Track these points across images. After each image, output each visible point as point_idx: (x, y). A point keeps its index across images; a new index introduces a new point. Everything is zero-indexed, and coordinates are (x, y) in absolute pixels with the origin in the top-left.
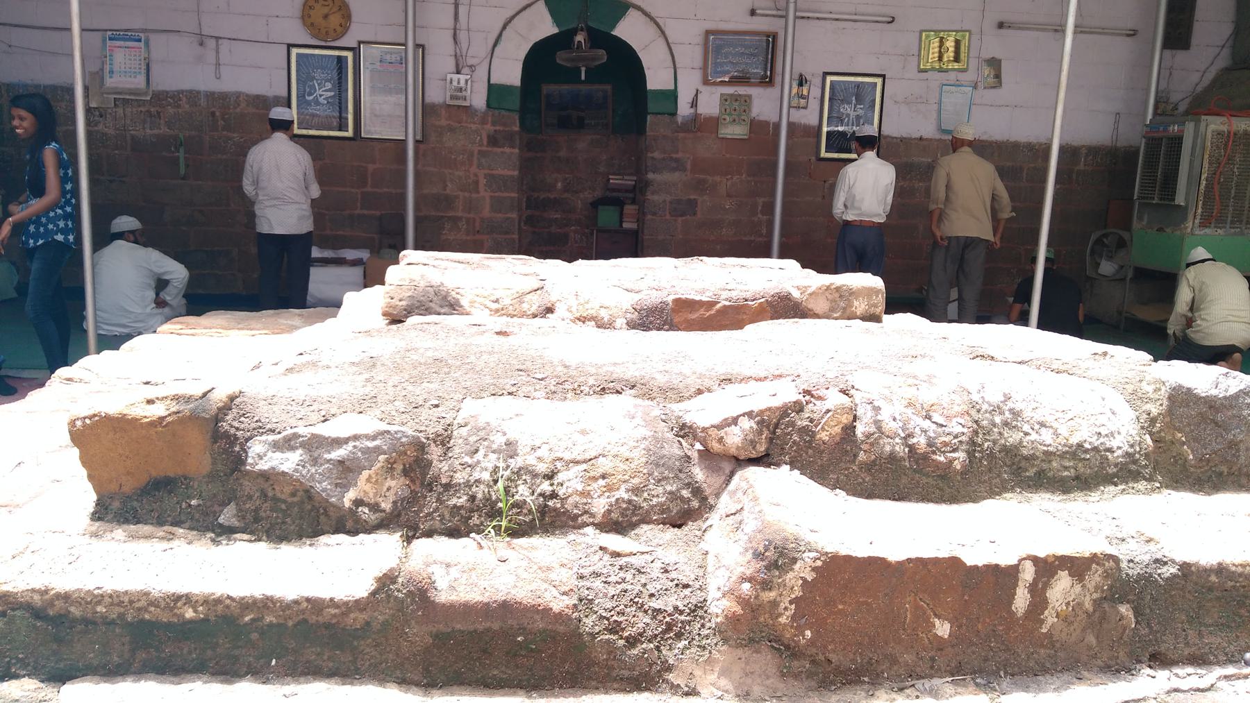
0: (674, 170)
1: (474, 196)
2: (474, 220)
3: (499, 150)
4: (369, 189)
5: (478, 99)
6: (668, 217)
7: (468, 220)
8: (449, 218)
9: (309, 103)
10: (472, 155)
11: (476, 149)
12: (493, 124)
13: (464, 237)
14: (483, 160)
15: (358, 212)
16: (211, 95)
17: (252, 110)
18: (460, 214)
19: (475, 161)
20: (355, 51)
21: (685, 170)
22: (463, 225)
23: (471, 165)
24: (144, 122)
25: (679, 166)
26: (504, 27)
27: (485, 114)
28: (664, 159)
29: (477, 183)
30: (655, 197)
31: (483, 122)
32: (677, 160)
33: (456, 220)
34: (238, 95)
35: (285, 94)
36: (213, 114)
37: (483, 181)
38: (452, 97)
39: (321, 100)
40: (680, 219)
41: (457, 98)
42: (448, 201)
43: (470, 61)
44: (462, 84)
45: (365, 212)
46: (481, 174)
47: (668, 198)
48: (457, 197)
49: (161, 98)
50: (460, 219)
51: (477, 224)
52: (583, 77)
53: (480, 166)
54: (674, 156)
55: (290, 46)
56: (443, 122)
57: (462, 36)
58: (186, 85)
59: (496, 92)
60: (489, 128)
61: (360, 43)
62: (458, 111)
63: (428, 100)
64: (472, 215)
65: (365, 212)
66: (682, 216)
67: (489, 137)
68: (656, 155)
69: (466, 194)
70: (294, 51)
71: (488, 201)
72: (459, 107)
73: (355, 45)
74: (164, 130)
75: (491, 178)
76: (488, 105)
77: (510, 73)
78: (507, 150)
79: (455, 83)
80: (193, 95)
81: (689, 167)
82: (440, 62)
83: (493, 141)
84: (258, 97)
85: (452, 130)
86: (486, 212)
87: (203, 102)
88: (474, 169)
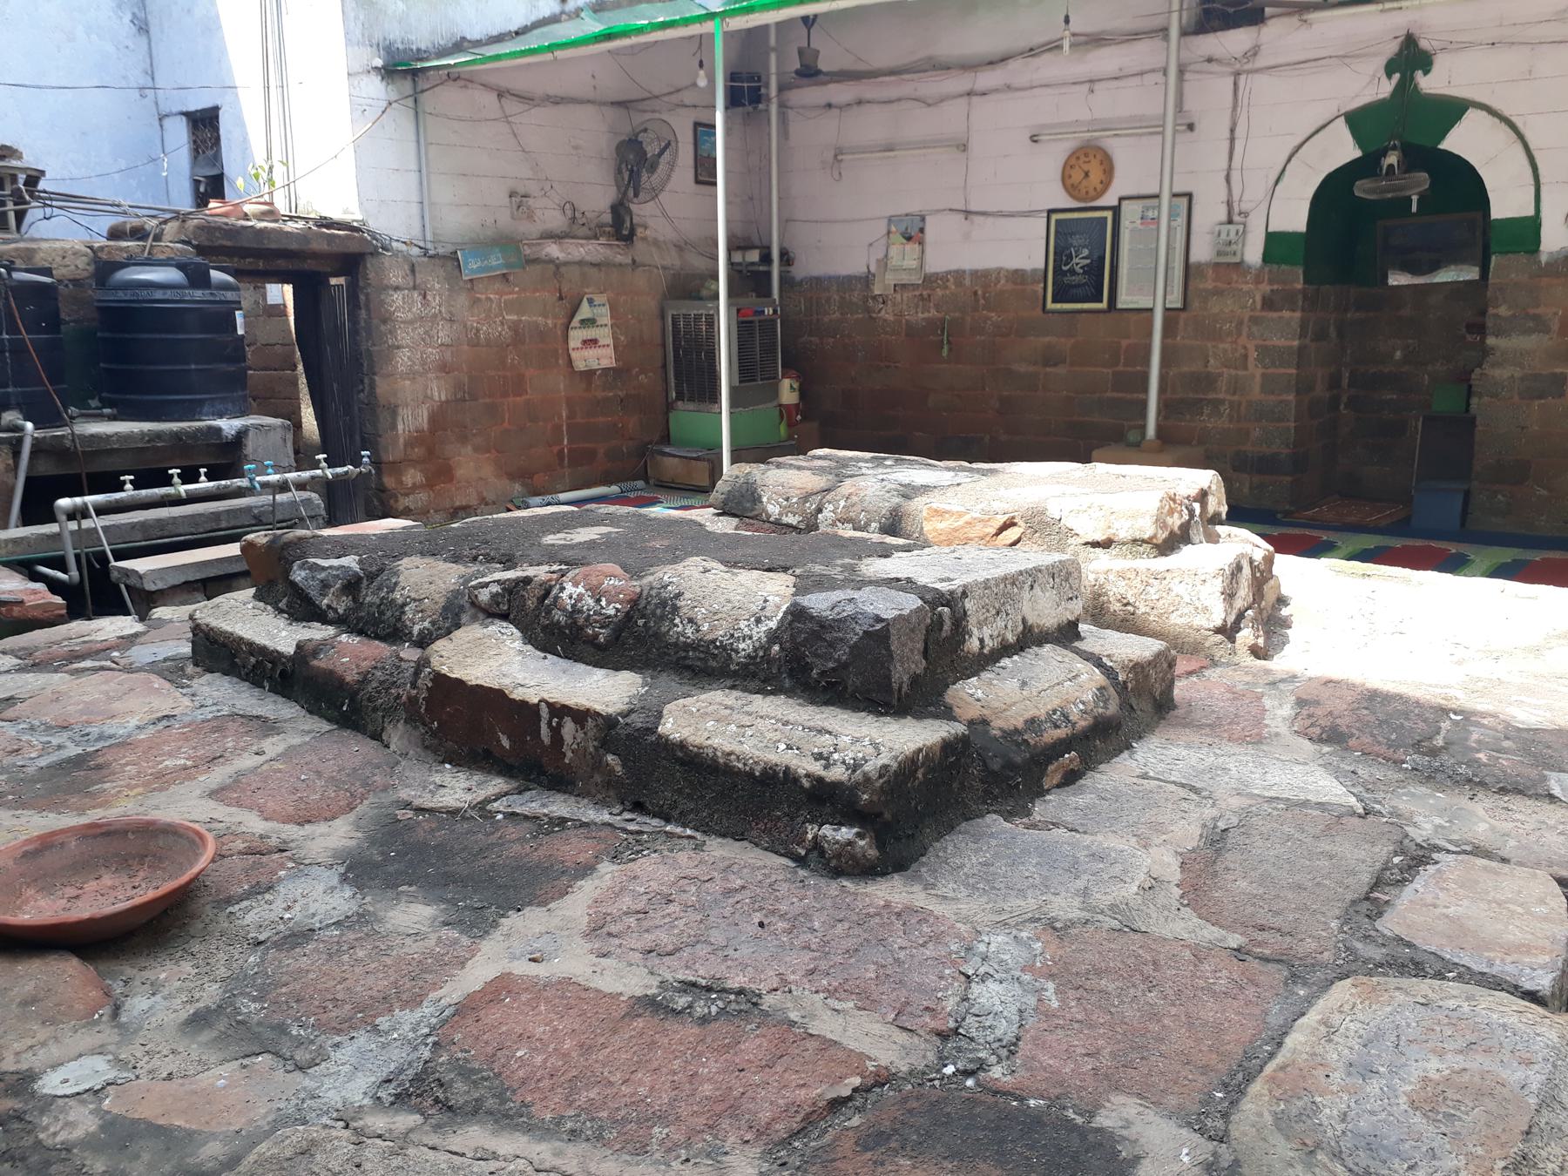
0: (1527, 332)
1: (1241, 373)
2: (1240, 404)
3: (1275, 315)
4: (1120, 368)
5: (1253, 253)
6: (1516, 398)
7: (1231, 403)
8: (1209, 401)
9: (1064, 273)
10: (1241, 323)
11: (1247, 314)
12: (1271, 282)
13: (1226, 426)
14: (1254, 329)
15: (1109, 394)
16: (975, 274)
17: (1010, 287)
18: (1221, 396)
19: (1245, 330)
20: (1116, 210)
21: (1547, 331)
22: (1225, 409)
23: (1239, 334)
24: (917, 306)
25: (1540, 325)
26: (1289, 160)
27: (1262, 268)
28: (1514, 316)
29: (1246, 357)
30: (1497, 373)
31: (1258, 280)
32: (1536, 318)
33: (1216, 403)
34: (999, 270)
35: (1042, 266)
36: (975, 293)
37: (1253, 354)
38: (1219, 253)
39: (1077, 269)
40: (1537, 402)
41: (1226, 254)
42: (1209, 381)
43: (1244, 207)
44: (1232, 236)
45: (1115, 395)
46: (1251, 347)
47: (1518, 373)
48: (1220, 375)
49: (931, 280)
50: (1222, 402)
51: (1243, 409)
52: (1414, 209)
53: (1250, 336)
54: (1532, 311)
55: (1050, 212)
56: (1209, 285)
57: (1235, 176)
58: (953, 267)
59: (1276, 243)
60: (1266, 288)
61: (1121, 199)
62: (1228, 268)
63: (1193, 259)
64: (1236, 398)
65: (1115, 395)
66: (1540, 397)
67: (1264, 298)
68: (1503, 311)
69: (1233, 372)
70: (1054, 217)
71: (1258, 379)
72: (1229, 264)
73: (1115, 203)
74: (933, 313)
75: (1264, 351)
76: (1267, 257)
77: (1294, 216)
78: (1286, 314)
79: (1223, 236)
80: (959, 275)
81: (1555, 326)
82: (1209, 214)
83: (1269, 303)
84: (1016, 271)
85: (1218, 293)
86: (1256, 392)
87: (967, 282)
88: (1243, 340)
